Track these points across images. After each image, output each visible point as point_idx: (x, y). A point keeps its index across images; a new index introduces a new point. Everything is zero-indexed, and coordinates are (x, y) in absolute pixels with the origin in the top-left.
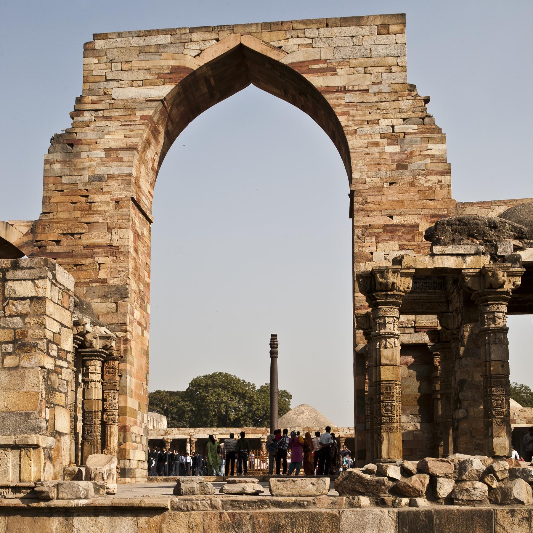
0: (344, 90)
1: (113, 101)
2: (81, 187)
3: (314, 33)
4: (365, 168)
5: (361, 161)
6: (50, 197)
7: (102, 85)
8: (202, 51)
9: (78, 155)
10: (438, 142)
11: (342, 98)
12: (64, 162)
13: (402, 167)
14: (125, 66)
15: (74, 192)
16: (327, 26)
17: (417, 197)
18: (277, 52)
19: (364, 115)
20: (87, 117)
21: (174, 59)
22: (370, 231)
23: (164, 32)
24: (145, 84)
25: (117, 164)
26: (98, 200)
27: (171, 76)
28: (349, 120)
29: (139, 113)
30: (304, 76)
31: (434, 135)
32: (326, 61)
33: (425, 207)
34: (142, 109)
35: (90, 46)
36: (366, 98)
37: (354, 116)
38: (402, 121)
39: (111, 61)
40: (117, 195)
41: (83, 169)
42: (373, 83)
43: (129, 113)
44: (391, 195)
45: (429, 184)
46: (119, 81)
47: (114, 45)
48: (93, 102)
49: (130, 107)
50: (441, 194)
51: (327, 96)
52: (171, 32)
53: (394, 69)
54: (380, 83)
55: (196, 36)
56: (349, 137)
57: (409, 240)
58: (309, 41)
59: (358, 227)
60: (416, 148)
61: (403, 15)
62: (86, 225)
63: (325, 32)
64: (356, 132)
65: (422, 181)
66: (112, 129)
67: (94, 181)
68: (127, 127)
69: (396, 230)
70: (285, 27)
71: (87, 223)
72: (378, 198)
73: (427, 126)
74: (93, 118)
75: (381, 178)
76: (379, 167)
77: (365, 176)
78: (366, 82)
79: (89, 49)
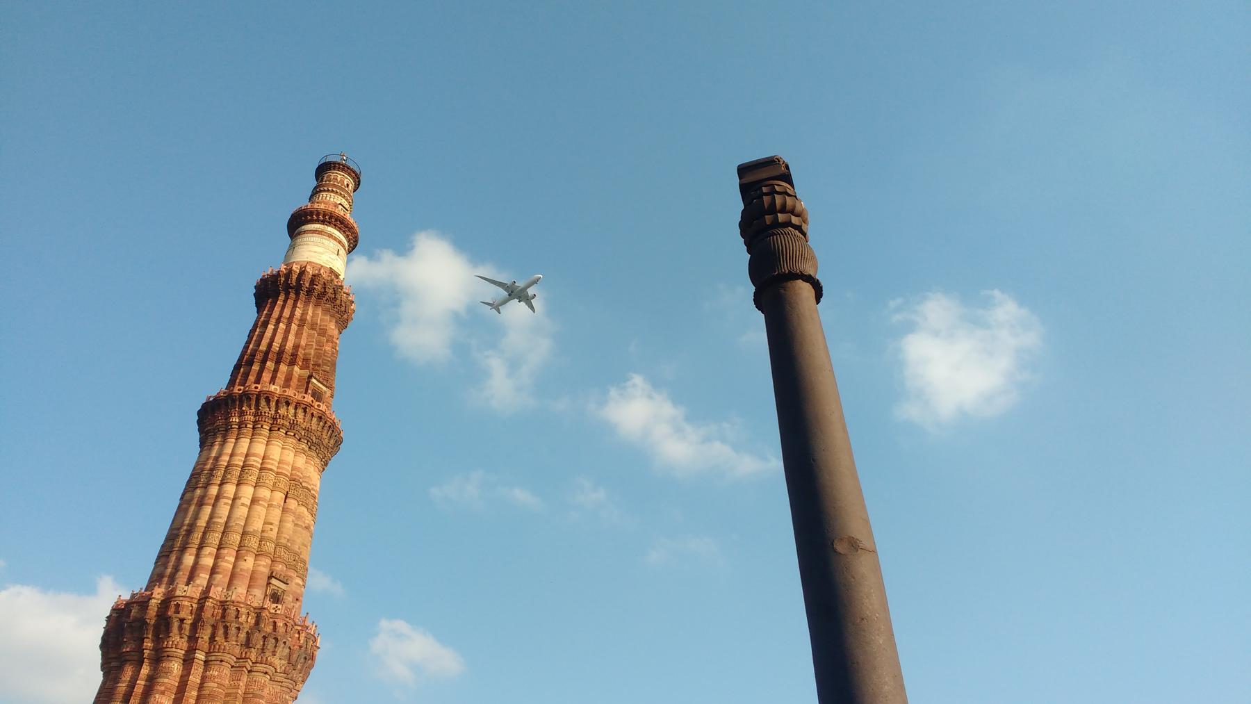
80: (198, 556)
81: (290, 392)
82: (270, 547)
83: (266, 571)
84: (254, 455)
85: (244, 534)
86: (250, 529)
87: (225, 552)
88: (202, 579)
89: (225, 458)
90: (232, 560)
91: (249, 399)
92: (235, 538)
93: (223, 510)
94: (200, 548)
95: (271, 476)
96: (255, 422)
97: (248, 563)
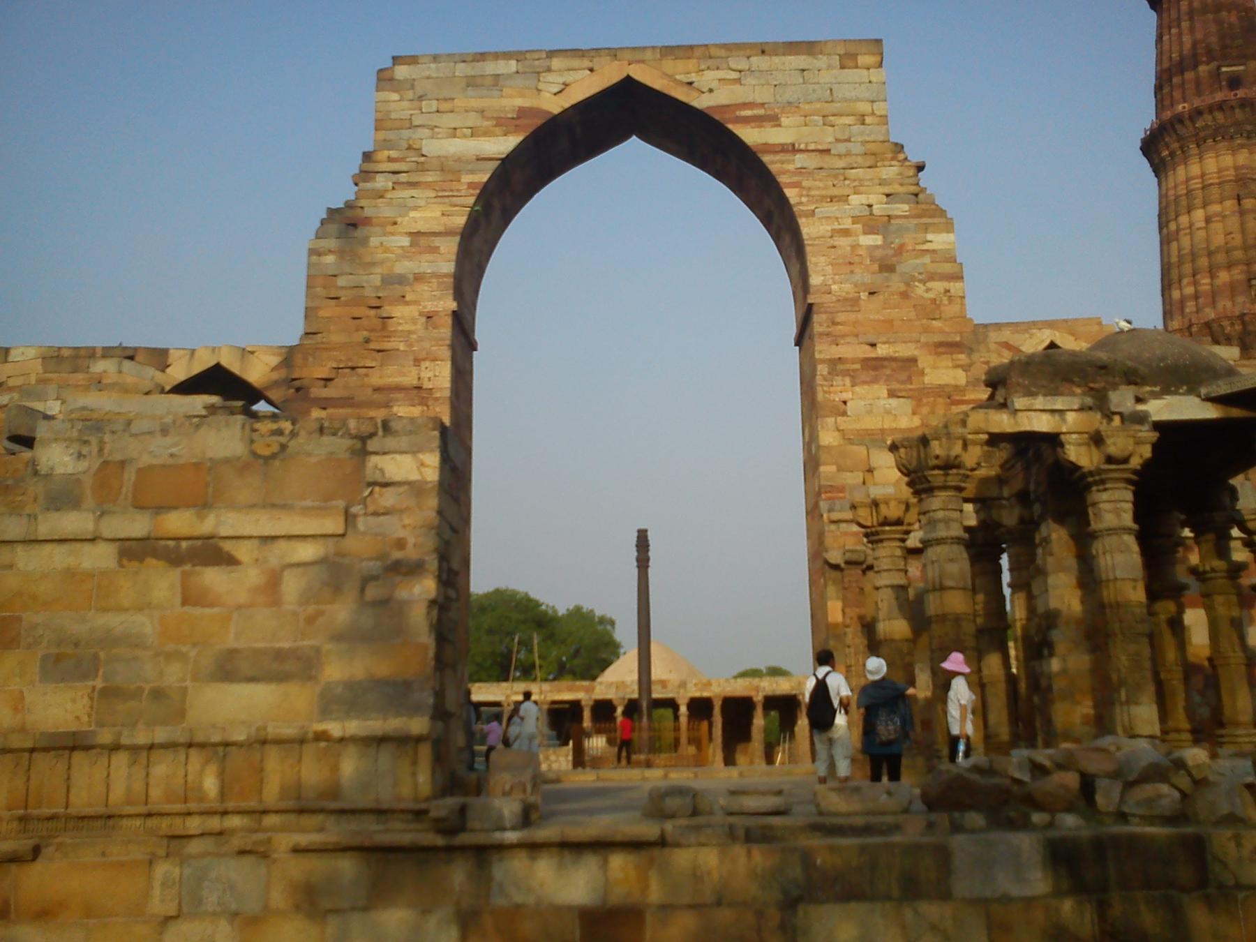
0: (792, 149)
1: (423, 159)
2: (369, 292)
3: (742, 64)
4: (829, 269)
5: (823, 259)
6: (317, 308)
7: (406, 133)
8: (566, 85)
9: (364, 242)
10: (940, 232)
11: (789, 162)
12: (341, 253)
13: (887, 268)
14: (445, 106)
15: (357, 301)
16: (763, 52)
17: (913, 315)
18: (685, 89)
19: (826, 188)
20: (381, 182)
21: (523, 96)
22: (840, 367)
23: (507, 55)
24: (475, 133)
25: (428, 257)
26: (398, 314)
27: (518, 122)
28: (801, 196)
29: (466, 179)
30: (730, 126)
31: (936, 220)
32: (763, 104)
33: (926, 330)
34: (472, 172)
35: (387, 75)
36: (828, 162)
37: (810, 189)
38: (885, 199)
39: (421, 98)
40: (430, 306)
41: (373, 264)
42: (838, 140)
43: (450, 177)
44: (872, 310)
45: (931, 295)
46: (432, 128)
47: (427, 73)
48: (390, 160)
49: (450, 169)
50: (951, 310)
51: (766, 159)
52: (519, 56)
53: (868, 120)
54: (848, 140)
55: (556, 63)
56: (802, 221)
57: (903, 382)
58: (735, 75)
59: (823, 361)
60: (909, 239)
61: (878, 42)
62: (375, 354)
63: (757, 61)
64: (813, 213)
65: (920, 289)
66: (422, 203)
67: (392, 284)
68: (447, 200)
69: (883, 367)
70: (698, 53)
71: (379, 351)
72: (852, 316)
73: (924, 206)
74: (390, 185)
75: (856, 286)
76: (852, 267)
77: (830, 282)
78: (827, 138)
79: (384, 79)
80: (1181, 289)
81: (1197, 102)
82: (1238, 254)
83: (1242, 277)
84: (1193, 178)
85: (1210, 254)
86: (1212, 248)
87: (1198, 277)
88: (1190, 307)
89: (1172, 192)
90: (1207, 281)
91: (1165, 129)
92: (1203, 262)
93: (1186, 242)
94: (1180, 281)
95: (1215, 191)
96: (1182, 148)
97: (1223, 277)
